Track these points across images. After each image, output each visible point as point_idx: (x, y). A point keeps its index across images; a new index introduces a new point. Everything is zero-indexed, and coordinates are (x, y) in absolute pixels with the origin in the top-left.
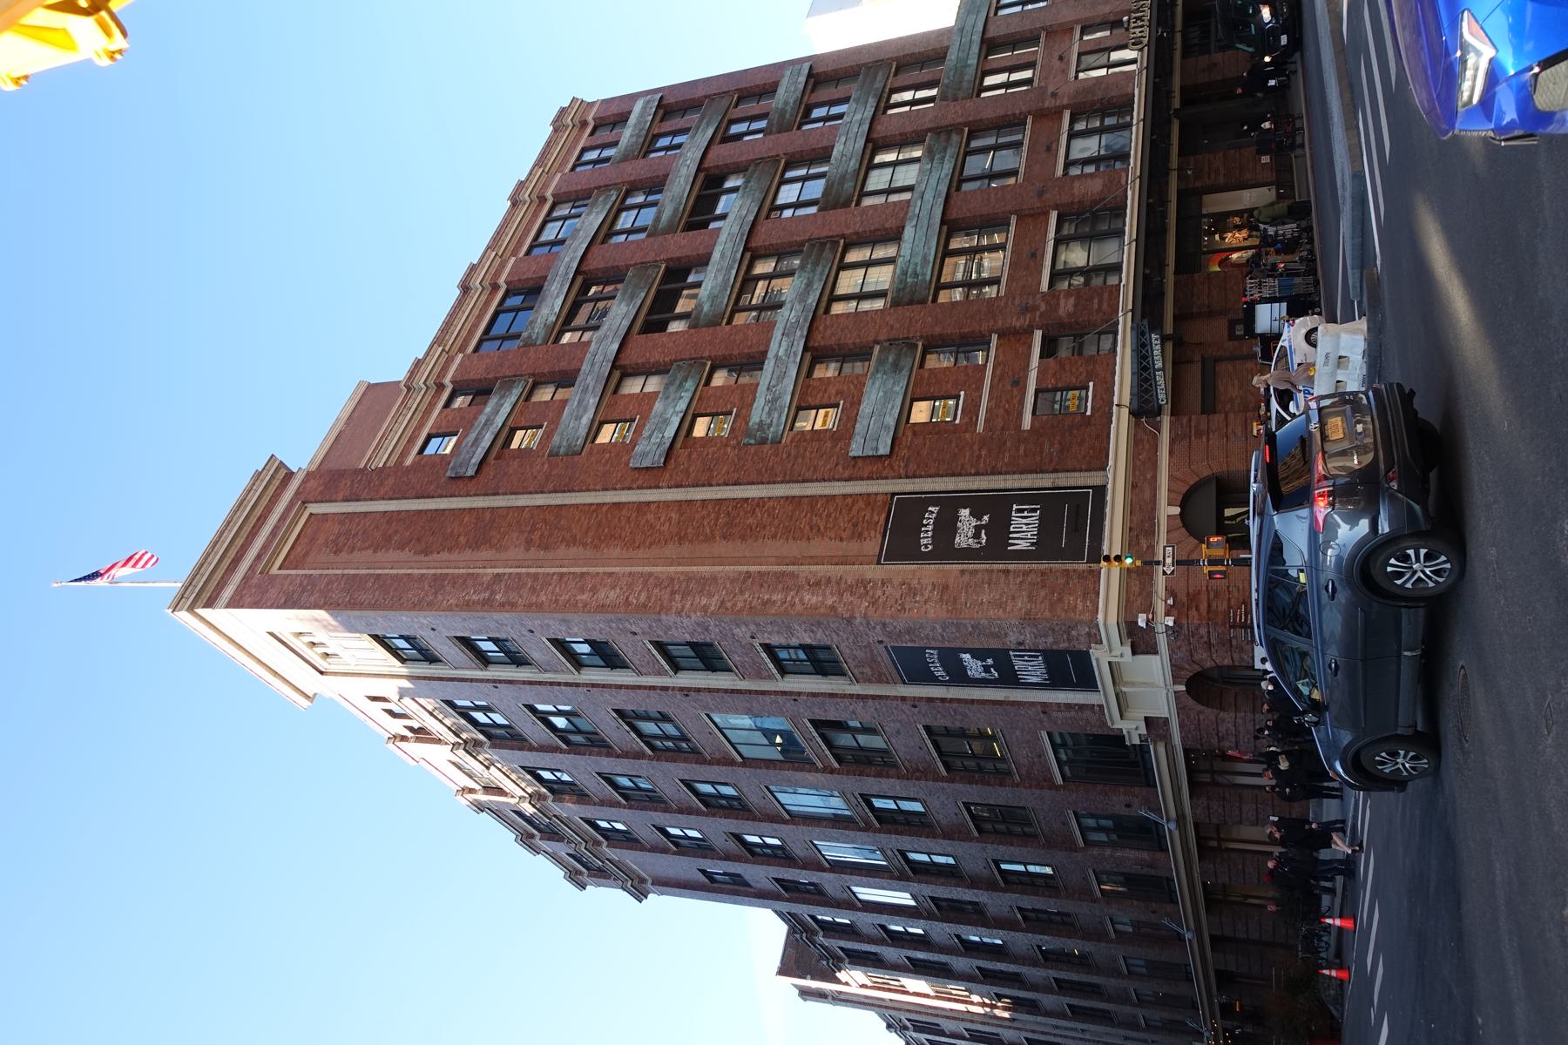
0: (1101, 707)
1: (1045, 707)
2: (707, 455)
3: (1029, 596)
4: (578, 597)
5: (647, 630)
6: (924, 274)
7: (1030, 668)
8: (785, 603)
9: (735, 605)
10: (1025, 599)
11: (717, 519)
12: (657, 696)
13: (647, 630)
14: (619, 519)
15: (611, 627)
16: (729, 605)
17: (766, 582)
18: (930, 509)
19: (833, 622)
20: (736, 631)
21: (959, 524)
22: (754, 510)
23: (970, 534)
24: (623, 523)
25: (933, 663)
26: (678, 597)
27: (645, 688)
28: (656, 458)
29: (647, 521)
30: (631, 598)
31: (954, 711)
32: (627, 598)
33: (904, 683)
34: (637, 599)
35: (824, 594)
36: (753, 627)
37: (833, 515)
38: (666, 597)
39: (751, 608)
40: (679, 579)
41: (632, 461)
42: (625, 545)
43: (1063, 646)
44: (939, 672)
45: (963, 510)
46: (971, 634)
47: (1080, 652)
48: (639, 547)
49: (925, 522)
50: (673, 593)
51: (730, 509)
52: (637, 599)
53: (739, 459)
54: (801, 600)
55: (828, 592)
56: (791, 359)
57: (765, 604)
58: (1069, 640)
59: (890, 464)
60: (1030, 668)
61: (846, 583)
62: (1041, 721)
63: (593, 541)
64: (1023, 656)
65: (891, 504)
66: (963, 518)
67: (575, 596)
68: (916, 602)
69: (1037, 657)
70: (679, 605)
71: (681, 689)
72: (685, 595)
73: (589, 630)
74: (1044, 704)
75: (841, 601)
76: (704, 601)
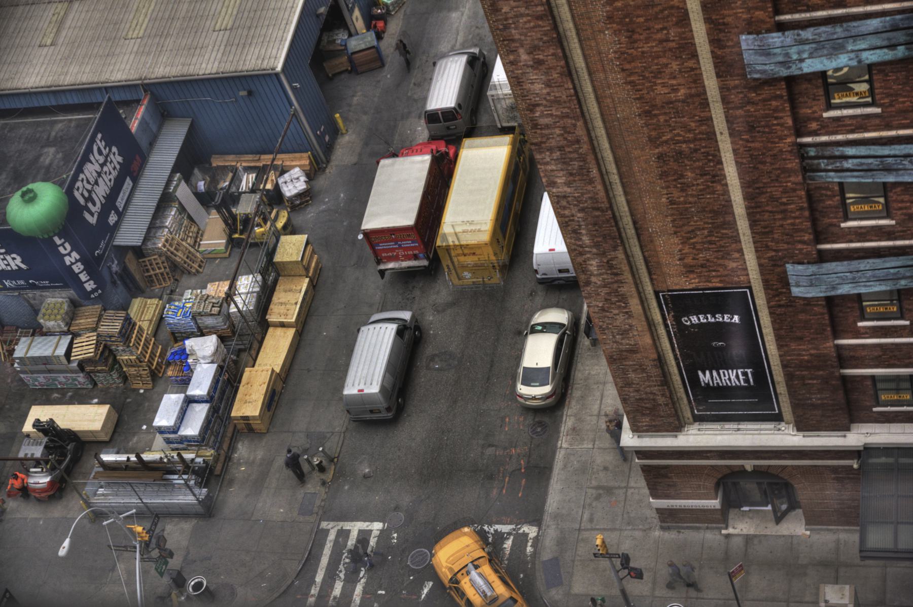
4: (521, 51)
9: (565, 208)
10: (638, 397)
11: (685, 142)
14: (662, 29)
24: (659, 36)
26: (557, 155)
28: (759, 68)
29: (666, 65)
30: (538, 109)
32: (538, 105)
34: (540, 117)
35: (601, 274)
38: (553, 143)
40: (580, 148)
42: (623, 53)
50: (561, 148)
51: (702, 150)
52: (542, 116)
53: (775, 155)
54: (589, 259)
55: (605, 276)
59: (781, 293)
61: (619, 287)
63: (617, 9)
67: (522, 46)
68: (614, 336)
70: (548, 159)
75: (599, 287)
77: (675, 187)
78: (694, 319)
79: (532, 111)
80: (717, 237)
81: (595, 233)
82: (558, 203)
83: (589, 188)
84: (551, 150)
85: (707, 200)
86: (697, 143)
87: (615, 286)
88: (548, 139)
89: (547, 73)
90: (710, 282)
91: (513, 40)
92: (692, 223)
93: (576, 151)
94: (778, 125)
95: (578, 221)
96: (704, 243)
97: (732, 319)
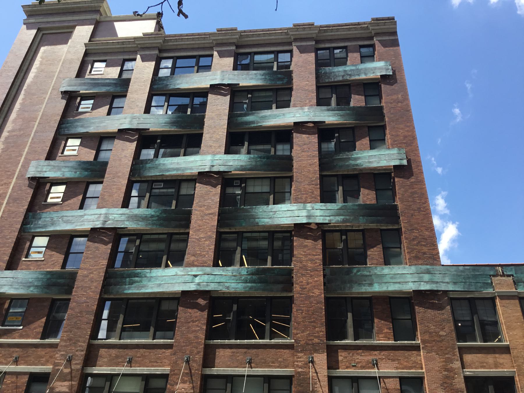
6: (129, 289)
56: (79, 224)
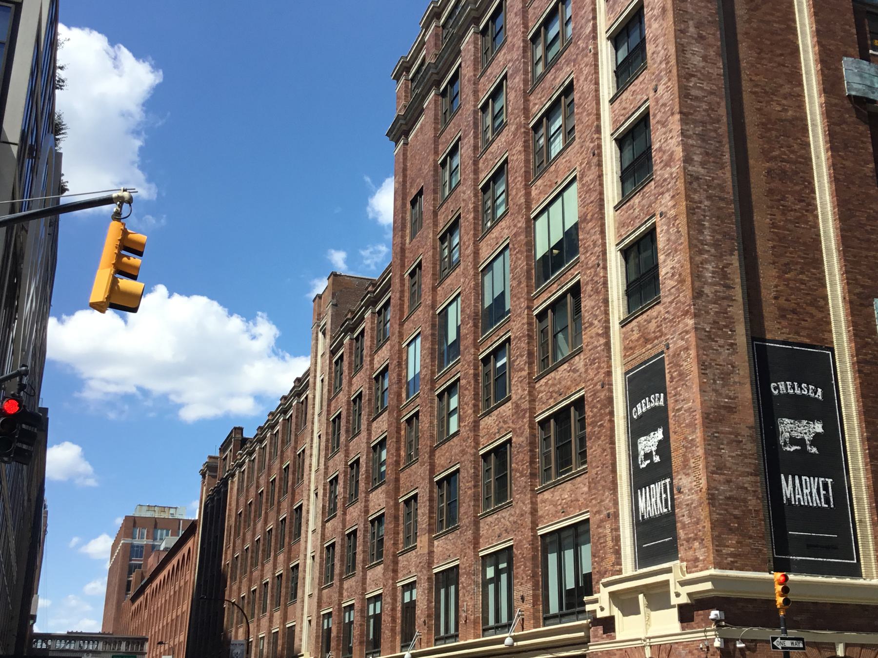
0: (620, 572)
1: (615, 516)
2: (863, 142)
3: (728, 498)
4: (691, 23)
5: (661, 102)
7: (653, 500)
8: (702, 244)
9: (695, 191)
10: (728, 494)
12: (590, 122)
13: (661, 102)
14: (782, 55)
15: (661, 63)
16: (695, 185)
17: (723, 222)
18: (819, 390)
19: (685, 296)
20: (667, 196)
21: (805, 422)
22: (803, 201)
23: (794, 434)
25: (650, 401)
27: (598, 109)
29: (781, 86)
30: (693, 79)
31: (601, 425)
32: (694, 76)
33: (626, 373)
34: (695, 86)
36: (672, 212)
37: (803, 287)
39: (694, 209)
41: (851, 59)
43: (681, 533)
44: (641, 409)
45: (820, 426)
46: (685, 438)
47: (676, 551)
48: (751, 80)
49: (804, 385)
50: (703, 123)
52: (695, 86)
57: (700, 223)
58: (688, 540)
59: (868, 343)
60: (653, 500)
62: (599, 512)
64: (665, 492)
65: (821, 348)
66: (812, 426)
69: (667, 507)
70: (691, 133)
71: (599, 147)
72: (702, 137)
73: (656, 40)
74: (616, 515)
76: (696, 158)
77: (778, 208)
78: (782, 385)
79: (688, 80)
80: (807, 276)
81: (717, 228)
82: (691, 183)
83: (720, 173)
84: (695, 122)
85: (802, 231)
86: (798, 165)
87: (725, 303)
88: (695, 111)
89: (705, 49)
90: (797, 333)
91: (686, 12)
92: (788, 254)
93: (715, 131)
94: (863, 148)
95: (704, 210)
96: (795, 280)
97: (815, 394)
